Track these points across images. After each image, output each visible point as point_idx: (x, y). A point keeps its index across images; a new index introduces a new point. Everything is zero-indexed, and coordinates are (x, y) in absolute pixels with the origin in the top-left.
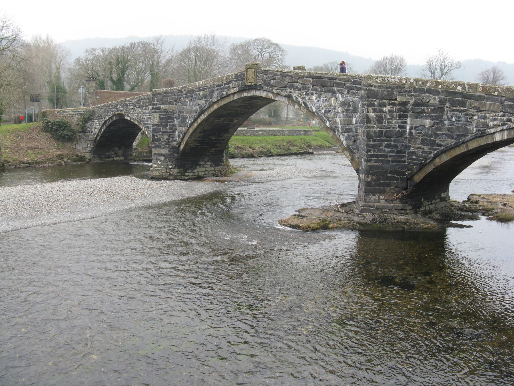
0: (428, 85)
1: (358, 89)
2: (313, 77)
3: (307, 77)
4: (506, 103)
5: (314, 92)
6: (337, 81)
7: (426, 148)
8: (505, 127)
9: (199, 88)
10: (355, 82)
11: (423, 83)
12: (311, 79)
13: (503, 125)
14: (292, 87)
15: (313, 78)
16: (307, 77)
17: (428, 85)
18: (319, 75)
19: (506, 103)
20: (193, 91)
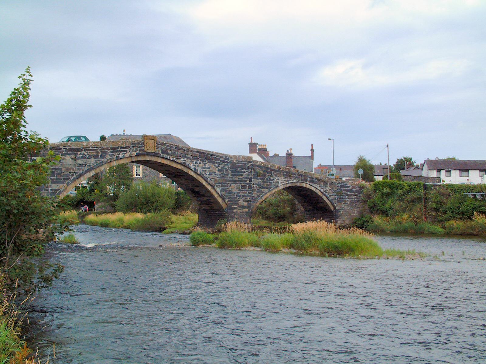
0: (258, 163)
1: (228, 163)
2: (200, 153)
3: (196, 152)
4: (284, 173)
5: (201, 162)
6: (215, 156)
7: (258, 194)
8: (284, 183)
9: (87, 148)
10: (226, 159)
11: (256, 162)
12: (198, 154)
13: (283, 182)
14: (186, 157)
15: (199, 153)
16: (196, 152)
17: (258, 163)
18: (204, 152)
19: (284, 173)
20: (78, 150)
